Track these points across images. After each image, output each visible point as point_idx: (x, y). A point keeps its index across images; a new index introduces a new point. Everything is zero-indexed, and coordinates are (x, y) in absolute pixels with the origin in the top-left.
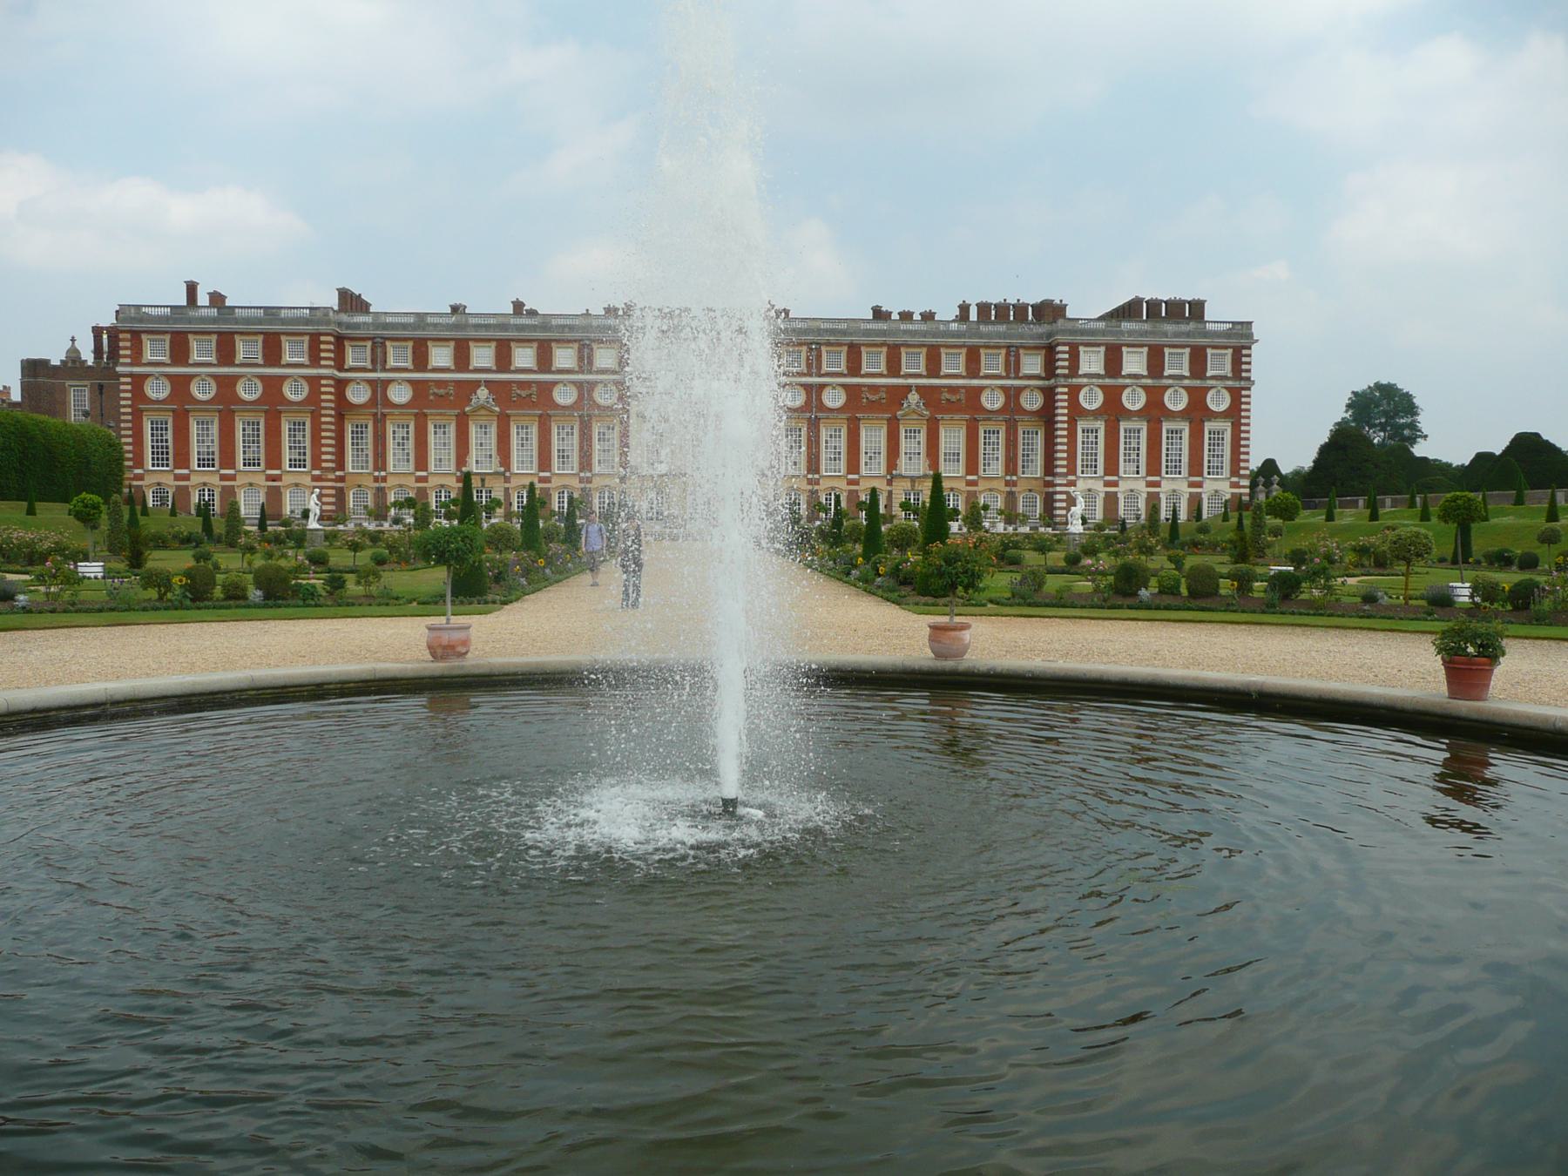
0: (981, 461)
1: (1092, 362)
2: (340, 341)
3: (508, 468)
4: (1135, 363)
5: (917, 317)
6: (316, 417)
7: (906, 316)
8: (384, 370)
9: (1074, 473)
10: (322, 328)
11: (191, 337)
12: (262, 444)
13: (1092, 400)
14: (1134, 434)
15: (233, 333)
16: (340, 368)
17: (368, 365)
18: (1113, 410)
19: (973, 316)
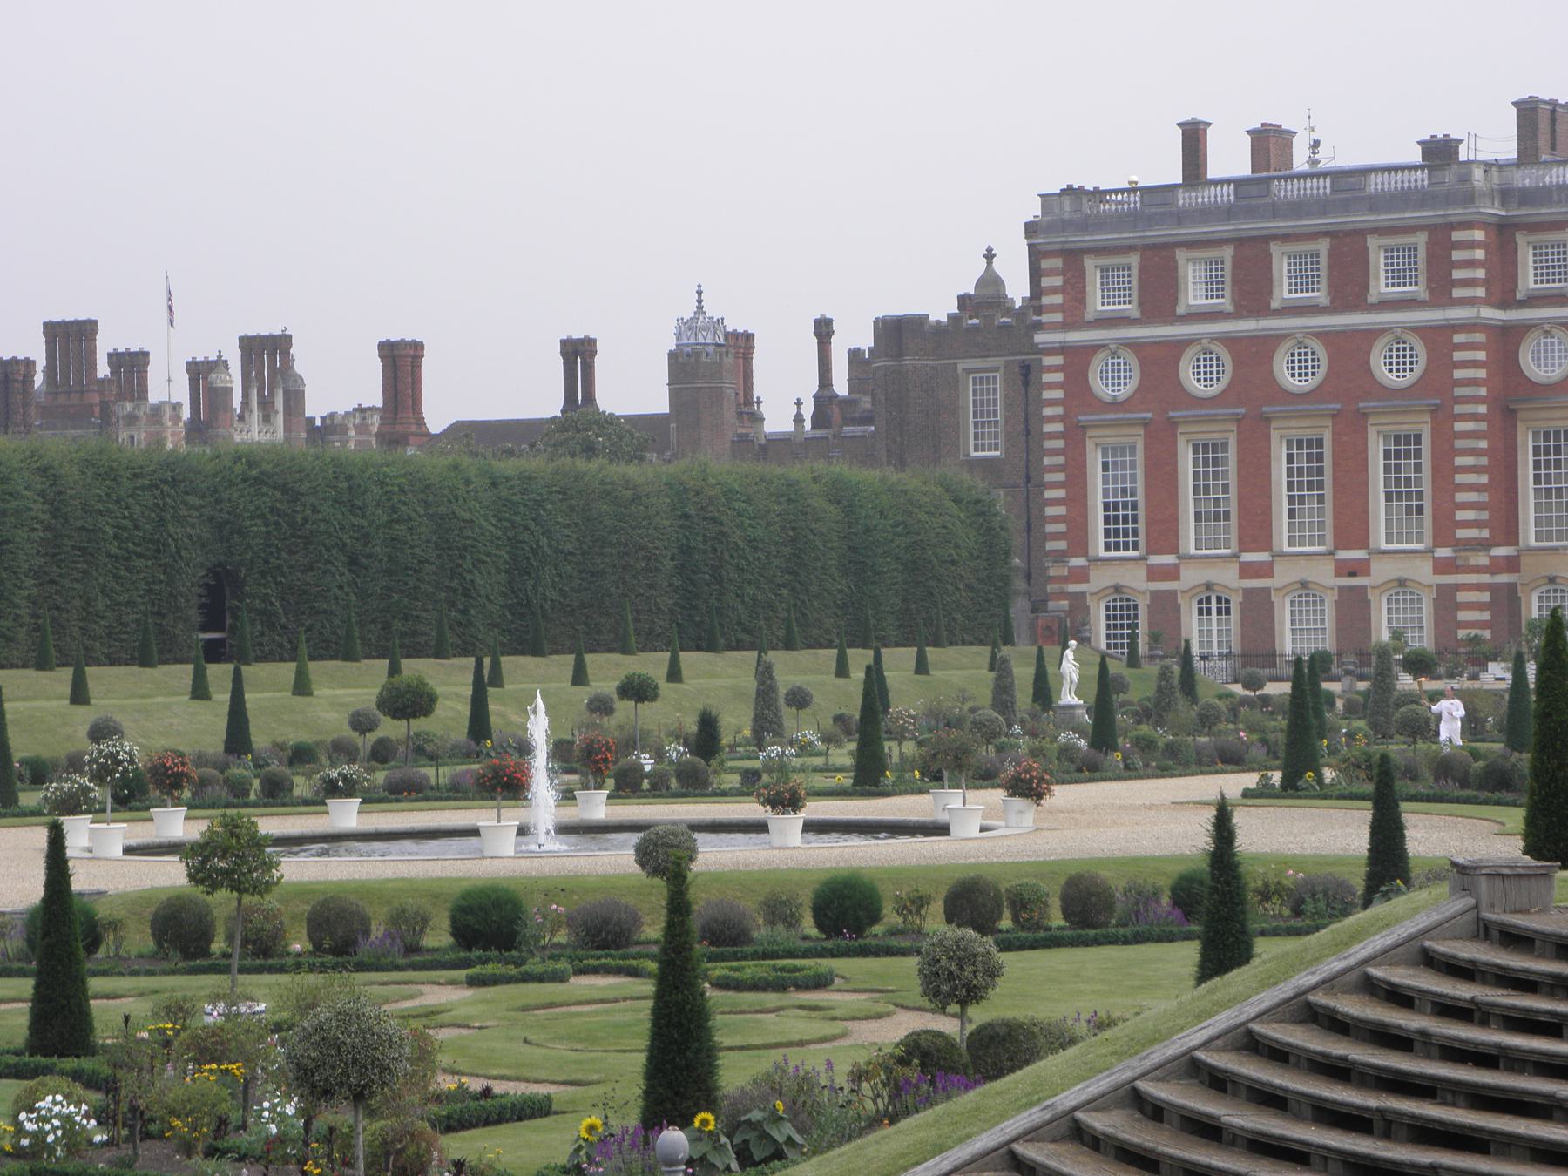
6: (1442, 417)
10: (1455, 212)
11: (1181, 255)
12: (1328, 492)
15: (1266, 239)
16: (1506, 299)
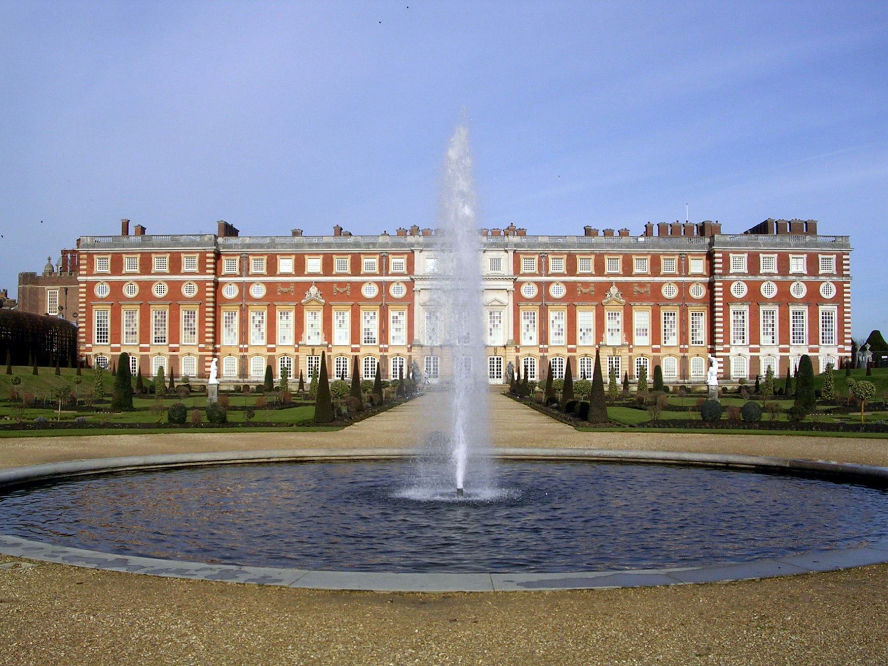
0: (663, 336)
1: (739, 264)
2: (218, 256)
3: (330, 342)
4: (769, 264)
6: (202, 307)
8: (248, 275)
9: (729, 343)
12: (167, 327)
13: (739, 290)
14: (770, 313)
17: (237, 272)
18: (754, 298)
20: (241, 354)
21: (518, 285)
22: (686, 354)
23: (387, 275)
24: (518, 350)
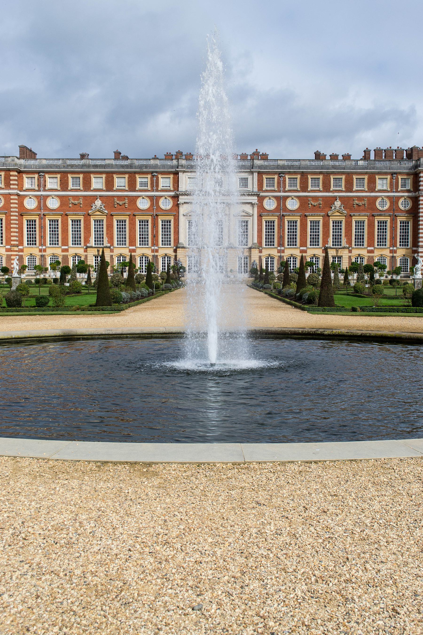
3: (112, 244)
5: (340, 158)
7: (334, 157)
8: (45, 190)
19: (372, 157)
20: (41, 254)
21: (261, 199)
22: (395, 255)
23: (157, 190)
24: (261, 252)
